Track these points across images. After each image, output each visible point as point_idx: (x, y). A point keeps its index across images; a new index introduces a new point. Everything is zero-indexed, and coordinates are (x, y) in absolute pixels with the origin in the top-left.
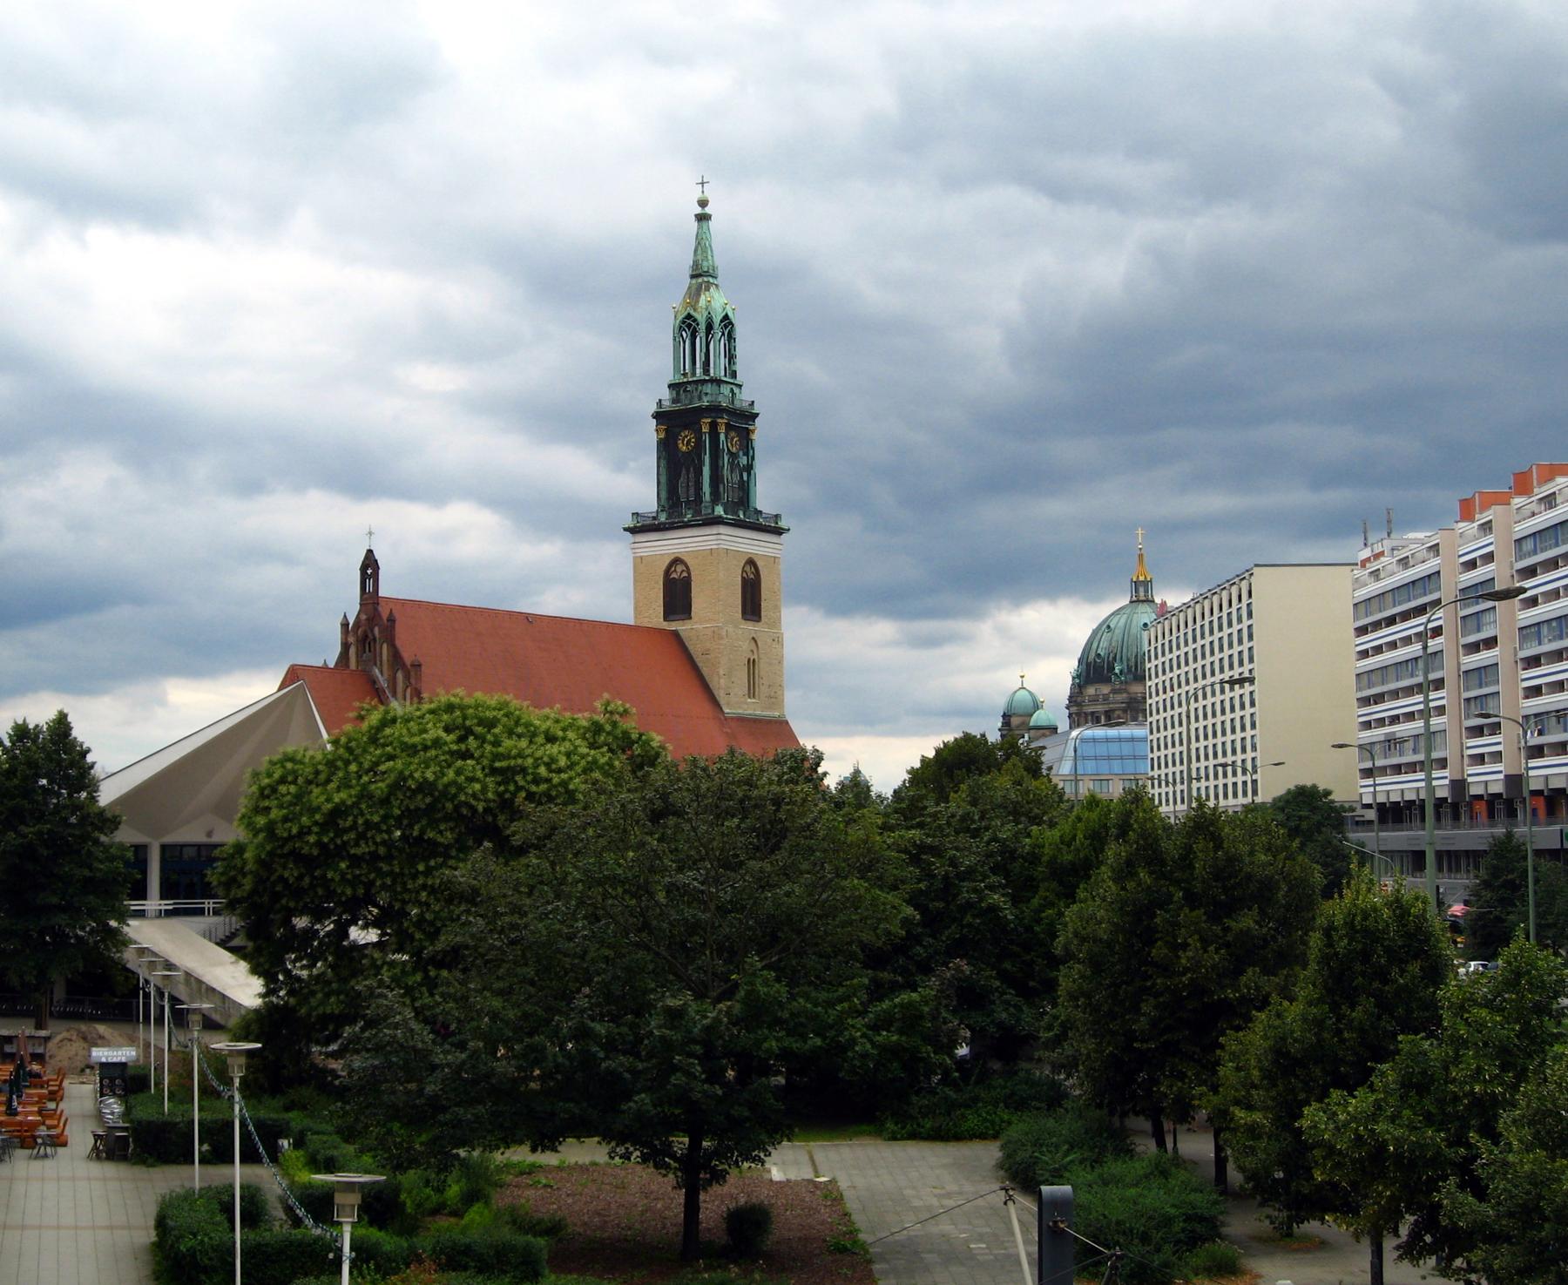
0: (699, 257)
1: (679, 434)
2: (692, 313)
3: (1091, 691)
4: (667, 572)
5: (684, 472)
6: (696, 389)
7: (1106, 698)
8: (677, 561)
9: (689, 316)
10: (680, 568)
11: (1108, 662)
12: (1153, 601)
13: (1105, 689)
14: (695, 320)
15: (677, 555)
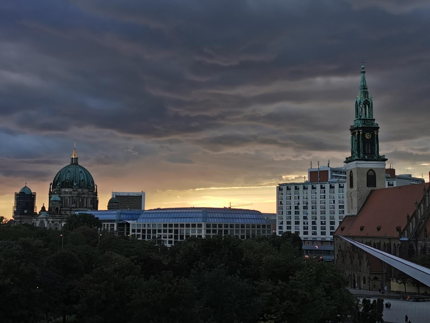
0: (364, 84)
1: (366, 133)
2: (368, 99)
3: (63, 190)
4: (368, 173)
5: (367, 144)
6: (371, 122)
7: (71, 193)
8: (371, 170)
9: (367, 100)
10: (371, 172)
11: (71, 182)
12: (77, 164)
13: (71, 190)
14: (368, 102)
15: (371, 168)
